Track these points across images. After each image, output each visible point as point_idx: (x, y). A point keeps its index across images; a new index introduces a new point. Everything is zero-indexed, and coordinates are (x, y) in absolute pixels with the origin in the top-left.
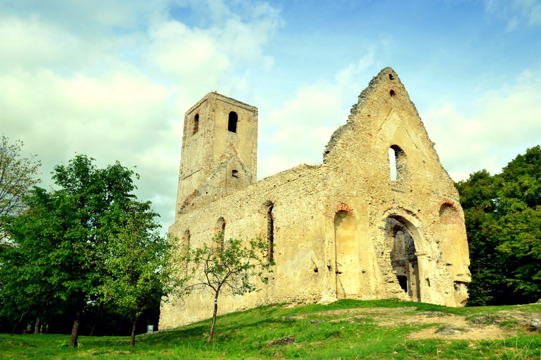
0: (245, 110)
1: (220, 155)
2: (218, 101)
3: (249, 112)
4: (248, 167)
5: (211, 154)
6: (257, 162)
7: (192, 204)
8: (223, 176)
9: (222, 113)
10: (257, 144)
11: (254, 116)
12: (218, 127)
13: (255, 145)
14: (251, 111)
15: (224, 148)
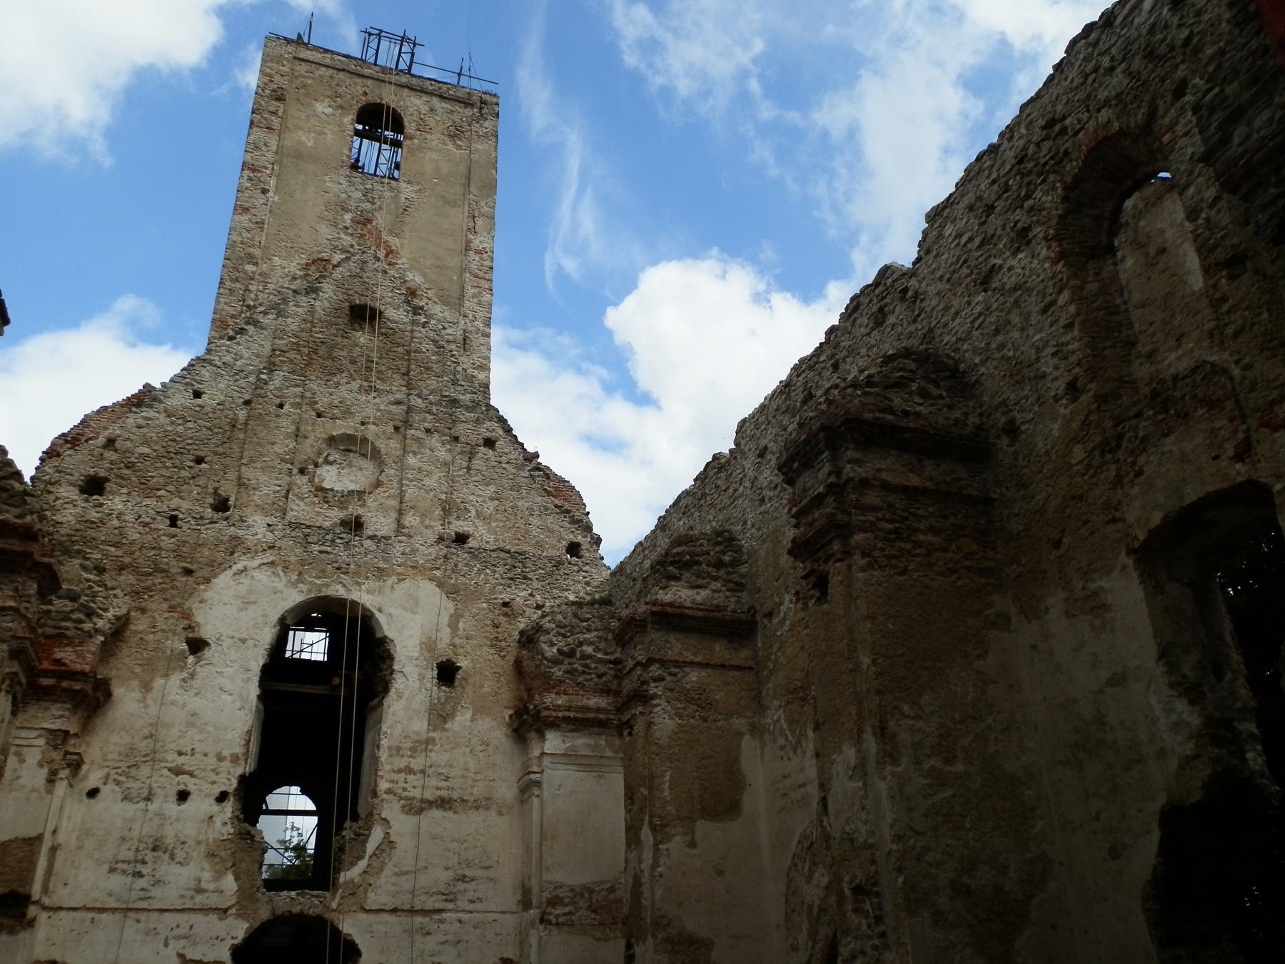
0: (435, 100)
1: (304, 259)
2: (302, 68)
3: (457, 108)
4: (446, 303)
5: (256, 252)
6: (495, 285)
7: (102, 440)
8: (292, 324)
9: (323, 108)
10: (492, 218)
11: (482, 117)
12: (299, 155)
13: (480, 222)
14: (467, 103)
15: (325, 231)
